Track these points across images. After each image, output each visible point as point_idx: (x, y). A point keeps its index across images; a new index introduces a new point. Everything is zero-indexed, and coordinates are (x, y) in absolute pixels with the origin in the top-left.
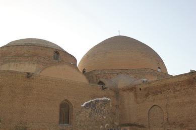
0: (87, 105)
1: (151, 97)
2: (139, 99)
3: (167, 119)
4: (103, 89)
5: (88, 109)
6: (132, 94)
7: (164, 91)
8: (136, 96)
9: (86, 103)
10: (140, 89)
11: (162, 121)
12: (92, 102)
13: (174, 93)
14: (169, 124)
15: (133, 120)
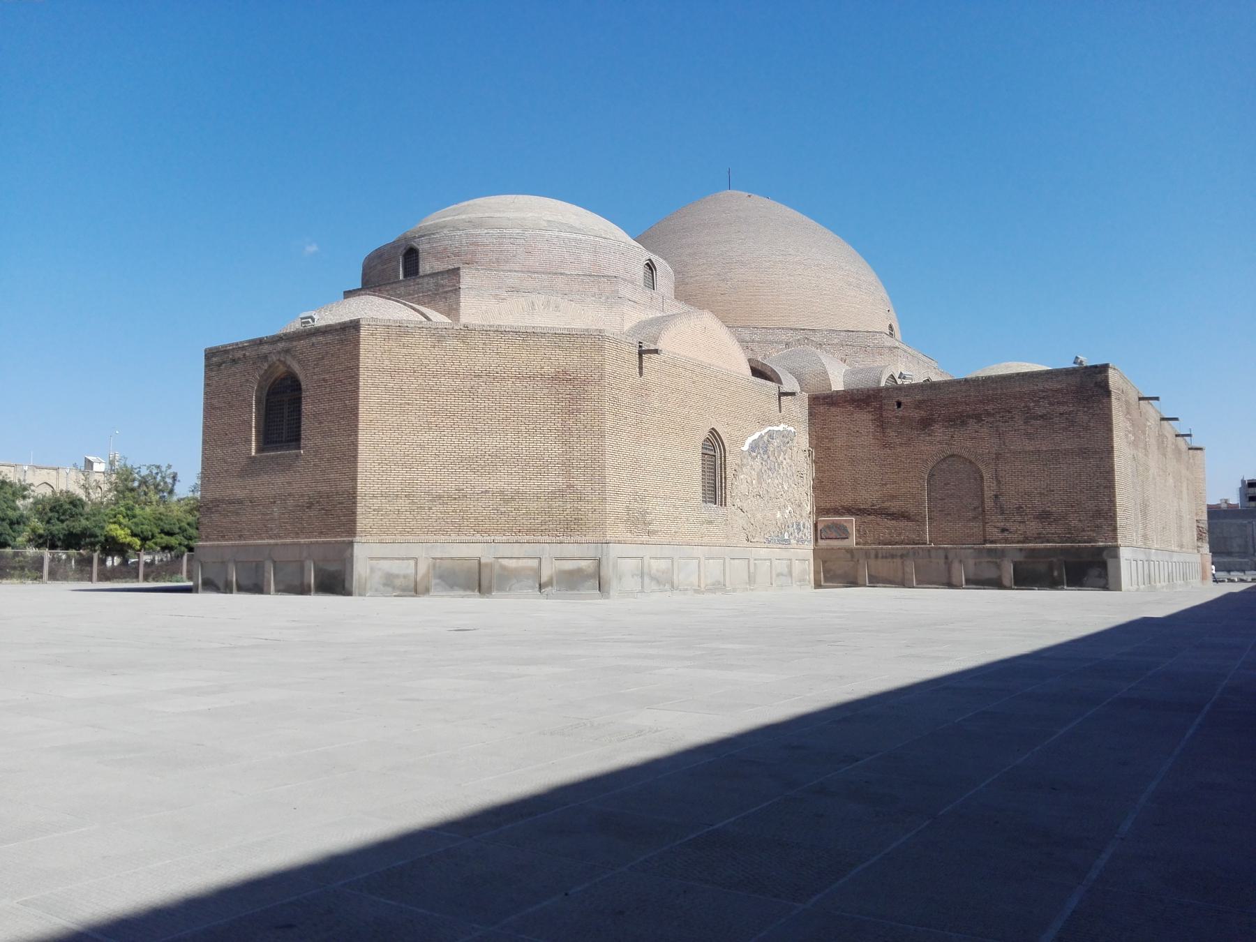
0: (753, 447)
1: (939, 431)
2: (891, 433)
3: (996, 496)
4: (782, 394)
5: (754, 458)
6: (864, 419)
7: (989, 414)
8: (882, 424)
9: (750, 440)
10: (899, 404)
11: (976, 503)
12: (761, 437)
13: (1026, 423)
14: (1002, 514)
15: (869, 496)
